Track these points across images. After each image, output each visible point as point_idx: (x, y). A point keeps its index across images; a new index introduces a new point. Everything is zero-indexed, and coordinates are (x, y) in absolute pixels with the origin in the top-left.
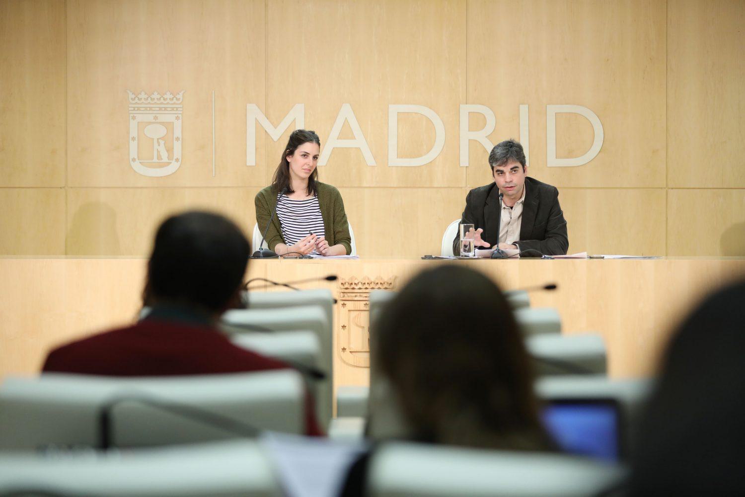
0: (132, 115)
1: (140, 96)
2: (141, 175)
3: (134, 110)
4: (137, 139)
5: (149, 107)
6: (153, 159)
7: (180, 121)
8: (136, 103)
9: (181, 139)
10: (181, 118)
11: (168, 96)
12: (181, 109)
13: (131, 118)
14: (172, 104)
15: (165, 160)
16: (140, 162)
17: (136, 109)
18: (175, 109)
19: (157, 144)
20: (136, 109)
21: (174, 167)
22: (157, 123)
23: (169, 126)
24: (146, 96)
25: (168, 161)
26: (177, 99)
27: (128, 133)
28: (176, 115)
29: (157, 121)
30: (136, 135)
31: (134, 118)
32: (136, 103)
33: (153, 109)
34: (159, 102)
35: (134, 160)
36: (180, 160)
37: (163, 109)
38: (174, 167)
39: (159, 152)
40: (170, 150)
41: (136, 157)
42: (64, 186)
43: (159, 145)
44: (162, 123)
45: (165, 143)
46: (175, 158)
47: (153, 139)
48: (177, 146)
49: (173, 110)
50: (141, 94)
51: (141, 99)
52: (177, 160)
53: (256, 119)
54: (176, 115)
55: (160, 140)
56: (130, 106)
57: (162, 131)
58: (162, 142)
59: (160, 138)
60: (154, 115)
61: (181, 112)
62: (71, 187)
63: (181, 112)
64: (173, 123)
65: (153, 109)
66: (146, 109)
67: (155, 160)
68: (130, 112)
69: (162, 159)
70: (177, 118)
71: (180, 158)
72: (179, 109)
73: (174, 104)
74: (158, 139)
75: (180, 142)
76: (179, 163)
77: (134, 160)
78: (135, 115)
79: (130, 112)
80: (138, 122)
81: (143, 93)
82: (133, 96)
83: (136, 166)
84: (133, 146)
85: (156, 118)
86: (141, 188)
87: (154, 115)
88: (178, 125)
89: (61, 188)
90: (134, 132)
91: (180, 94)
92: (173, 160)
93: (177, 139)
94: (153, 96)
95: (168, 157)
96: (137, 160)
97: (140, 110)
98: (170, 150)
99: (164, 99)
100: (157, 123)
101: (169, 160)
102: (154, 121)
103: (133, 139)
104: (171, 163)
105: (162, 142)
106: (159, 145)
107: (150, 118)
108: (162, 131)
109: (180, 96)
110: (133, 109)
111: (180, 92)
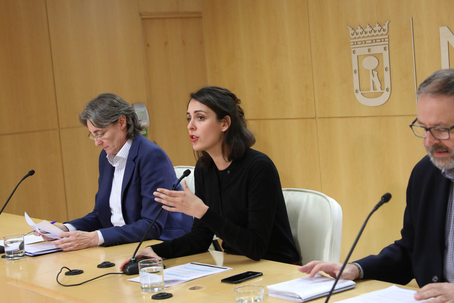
0: (353, 50)
1: (357, 31)
2: (364, 105)
3: (354, 44)
4: (357, 72)
5: (365, 41)
6: (369, 90)
7: (387, 51)
8: (355, 38)
9: (389, 69)
10: (388, 48)
11: (377, 28)
12: (387, 40)
13: (353, 52)
14: (382, 35)
15: (379, 90)
16: (361, 93)
17: (355, 43)
18: (383, 40)
19: (372, 75)
20: (355, 43)
21: (386, 95)
22: (371, 55)
23: (378, 56)
24: (361, 30)
25: (382, 91)
26: (384, 30)
27: (352, 66)
28: (384, 46)
29: (371, 53)
30: (357, 69)
31: (354, 52)
32: (355, 38)
33: (367, 42)
34: (370, 35)
35: (357, 91)
36: (390, 90)
37: (374, 41)
38: (386, 95)
39: (374, 82)
40: (381, 81)
41: (358, 89)
42: (314, 116)
43: (373, 76)
44: (374, 55)
45: (377, 74)
46: (386, 87)
47: (369, 70)
48: (387, 75)
49: (381, 41)
50: (357, 29)
51: (358, 33)
52: (387, 90)
53: (448, 42)
54: (384, 46)
55: (374, 71)
56: (352, 41)
57: (374, 63)
58: (375, 73)
59: (374, 70)
60: (368, 48)
61: (387, 43)
62: (320, 118)
63: (387, 43)
64: (382, 53)
65: (367, 42)
66: (362, 42)
67: (372, 91)
68: (352, 47)
69: (377, 89)
70: (385, 49)
71: (389, 87)
72: (386, 40)
73: (382, 35)
74: (372, 70)
75: (389, 71)
76: (389, 92)
77: (357, 91)
78: (355, 49)
79: (352, 47)
80: (358, 56)
81: (359, 28)
82: (353, 32)
83: (359, 96)
84: (356, 77)
85: (369, 50)
86: (365, 117)
87: (368, 48)
88: (386, 54)
89: (313, 118)
90: (355, 67)
91: (385, 24)
92: (384, 90)
93: (386, 69)
94: (366, 30)
95: (381, 87)
96: (359, 91)
97: (359, 44)
98: (381, 81)
99: (375, 32)
100: (371, 55)
101: (382, 90)
102: (368, 53)
103: (355, 72)
104: (383, 92)
105: (375, 73)
106: (373, 76)
107: (364, 51)
108: (374, 63)
109: (385, 27)
110: (353, 44)
111: (386, 23)
